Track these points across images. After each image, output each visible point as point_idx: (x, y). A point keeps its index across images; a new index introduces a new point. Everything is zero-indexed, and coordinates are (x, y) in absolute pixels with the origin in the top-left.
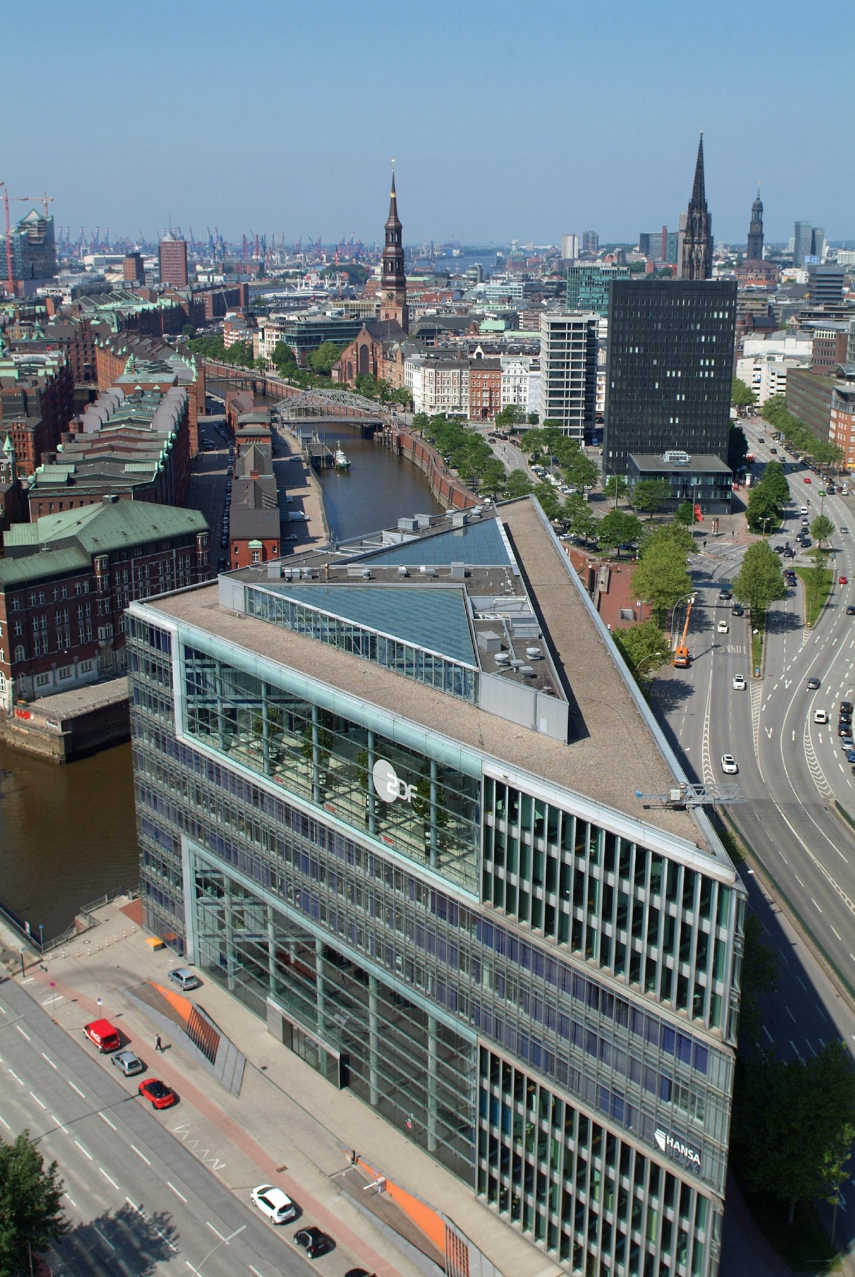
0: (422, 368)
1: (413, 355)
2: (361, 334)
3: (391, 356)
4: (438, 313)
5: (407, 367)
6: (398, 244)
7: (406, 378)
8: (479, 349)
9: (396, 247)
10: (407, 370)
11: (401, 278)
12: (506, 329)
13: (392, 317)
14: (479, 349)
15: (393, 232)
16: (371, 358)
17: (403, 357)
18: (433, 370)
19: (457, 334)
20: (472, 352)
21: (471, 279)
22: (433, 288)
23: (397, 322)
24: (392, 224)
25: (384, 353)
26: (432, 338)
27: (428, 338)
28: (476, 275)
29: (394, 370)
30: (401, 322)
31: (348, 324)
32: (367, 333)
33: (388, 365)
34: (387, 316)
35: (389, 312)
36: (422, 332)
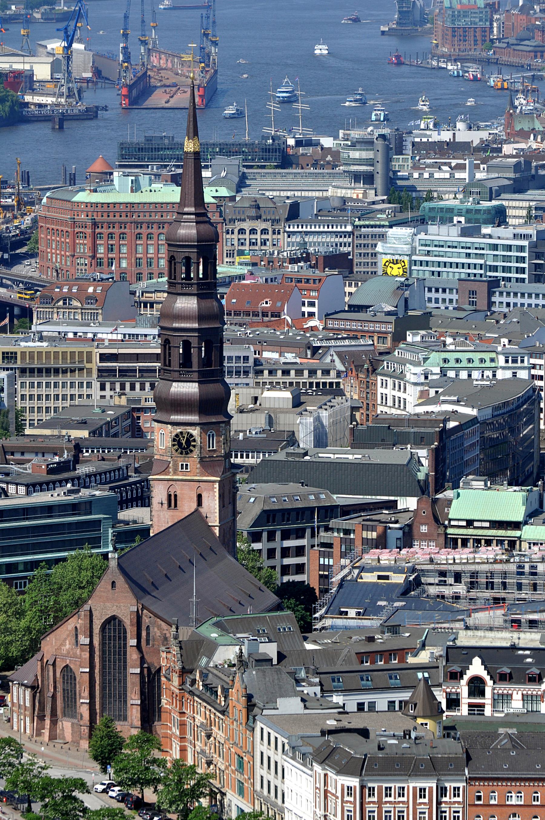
0: (317, 768)
1: (280, 702)
2: (103, 586)
3: (210, 689)
4: (297, 403)
5: (266, 742)
6: (208, 287)
7: (260, 771)
8: (476, 668)
9: (200, 296)
10: (260, 747)
11: (214, 388)
12: (532, 515)
13: (187, 507)
14: (476, 668)
15: (193, 253)
16: (133, 656)
17: (250, 706)
18: (354, 782)
19: (381, 543)
20: (456, 676)
21: (357, 177)
22: (247, 225)
23: (203, 520)
24: (188, 230)
25: (184, 672)
26: (300, 534)
27: (286, 536)
28: (370, 162)
29: (219, 734)
30: (214, 520)
31: (48, 510)
32: (121, 581)
33: (200, 714)
34: (172, 501)
35: (178, 488)
36: (268, 516)
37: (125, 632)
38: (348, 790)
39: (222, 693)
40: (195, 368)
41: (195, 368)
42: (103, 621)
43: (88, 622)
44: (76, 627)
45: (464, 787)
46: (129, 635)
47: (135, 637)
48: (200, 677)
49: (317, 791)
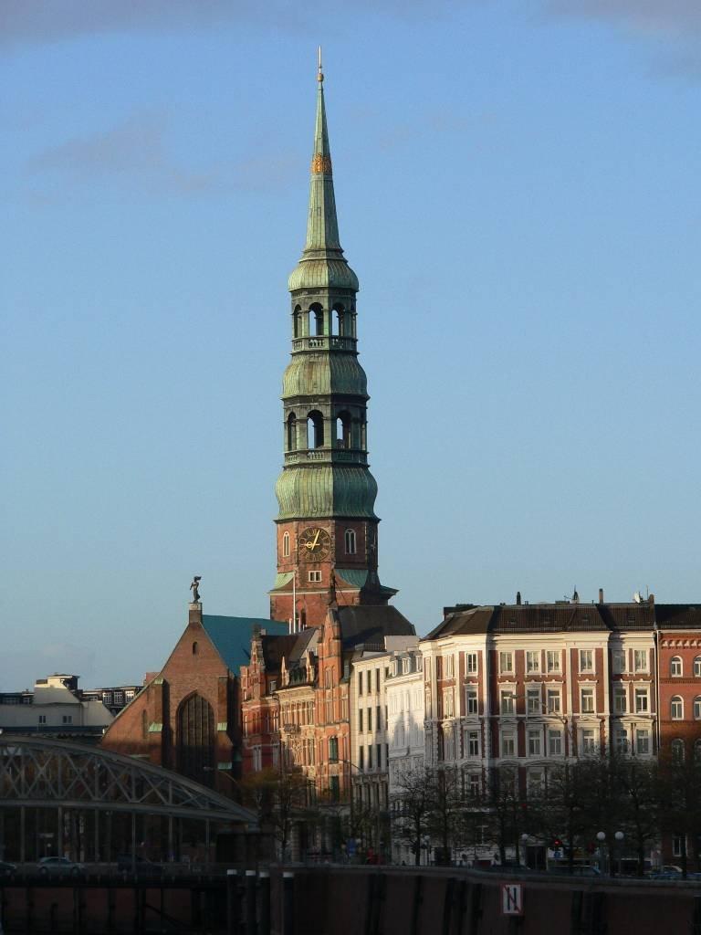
37: (211, 714)
38: (470, 661)
39: (311, 664)
40: (328, 443)
41: (328, 443)
42: (180, 700)
43: (161, 700)
44: (145, 711)
45: (652, 650)
46: (216, 718)
47: (225, 718)
48: (286, 668)
49: (428, 689)
